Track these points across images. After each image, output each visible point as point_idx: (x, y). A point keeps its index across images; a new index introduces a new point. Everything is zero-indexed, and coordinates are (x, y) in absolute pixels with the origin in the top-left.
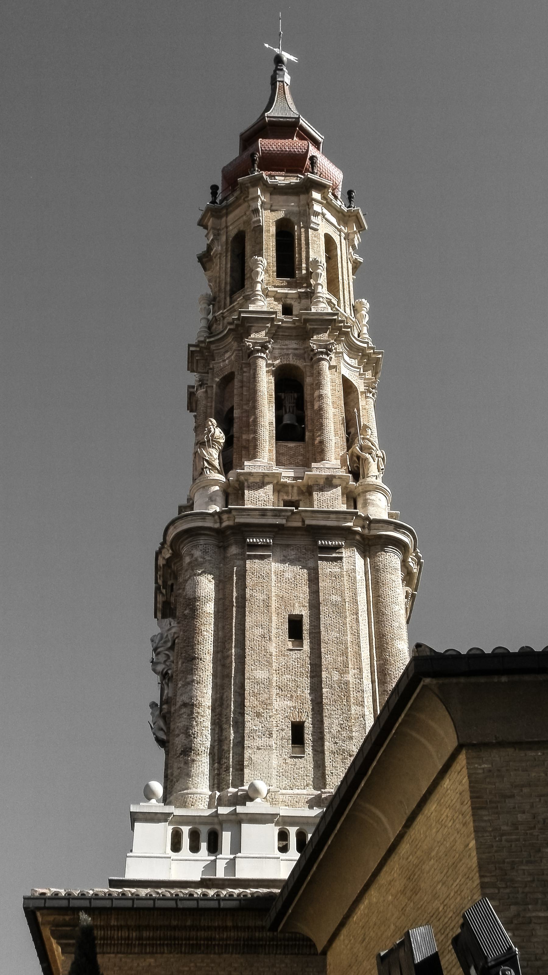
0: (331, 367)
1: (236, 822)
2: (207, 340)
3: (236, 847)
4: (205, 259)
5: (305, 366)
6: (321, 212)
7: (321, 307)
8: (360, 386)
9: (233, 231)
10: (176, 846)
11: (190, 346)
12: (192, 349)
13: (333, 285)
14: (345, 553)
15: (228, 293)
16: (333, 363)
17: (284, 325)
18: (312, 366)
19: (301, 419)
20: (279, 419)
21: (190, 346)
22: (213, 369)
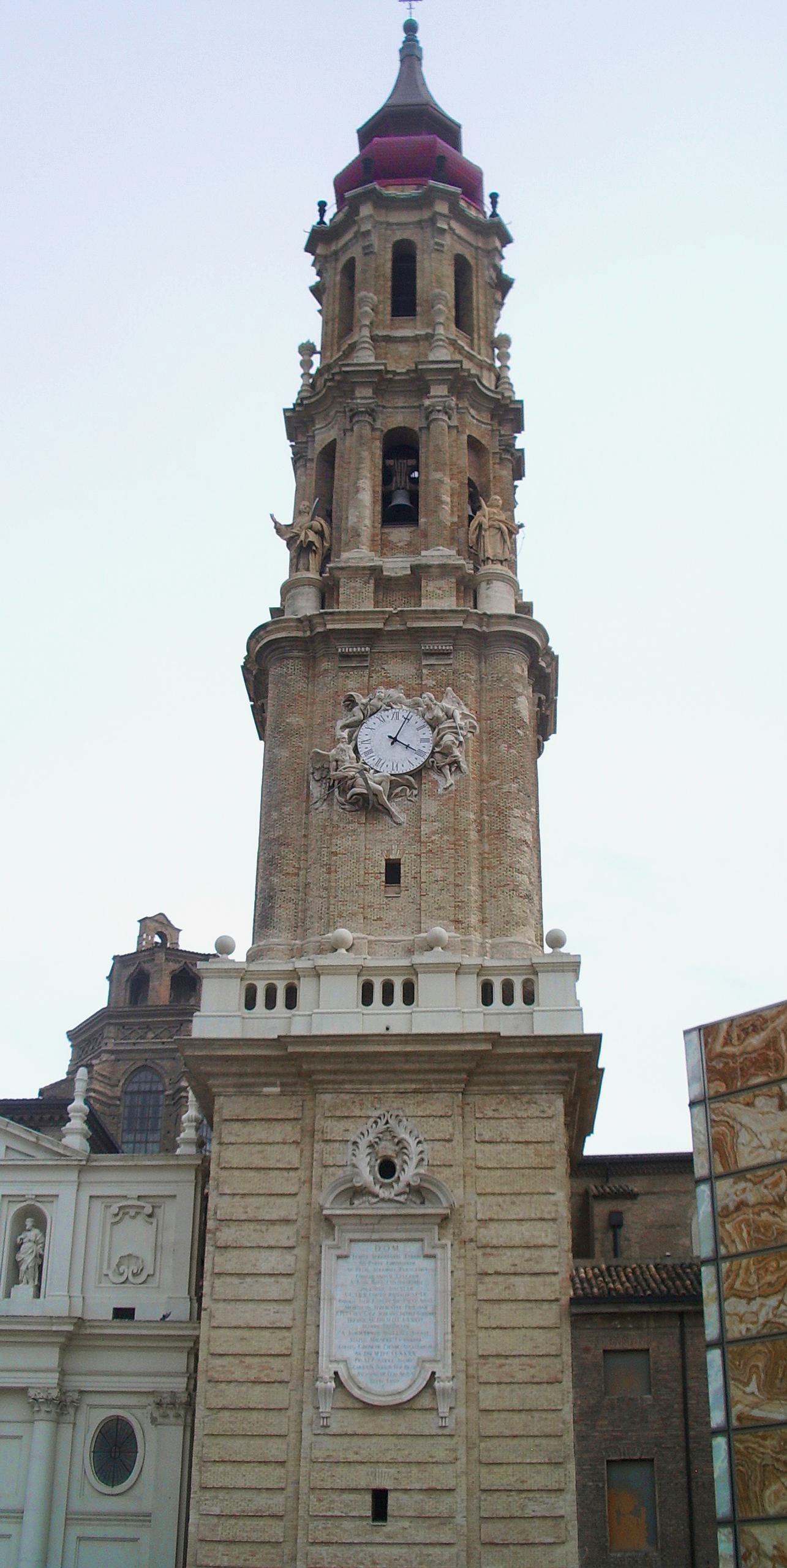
0: (449, 427)
2: (305, 402)
4: (317, 291)
5: (421, 429)
6: (446, 227)
7: (442, 354)
9: (344, 259)
10: (250, 1004)
11: (285, 410)
12: (288, 414)
13: (462, 319)
15: (335, 340)
16: (454, 422)
17: (397, 378)
18: (428, 428)
19: (414, 497)
20: (386, 498)
21: (285, 410)
22: (314, 437)
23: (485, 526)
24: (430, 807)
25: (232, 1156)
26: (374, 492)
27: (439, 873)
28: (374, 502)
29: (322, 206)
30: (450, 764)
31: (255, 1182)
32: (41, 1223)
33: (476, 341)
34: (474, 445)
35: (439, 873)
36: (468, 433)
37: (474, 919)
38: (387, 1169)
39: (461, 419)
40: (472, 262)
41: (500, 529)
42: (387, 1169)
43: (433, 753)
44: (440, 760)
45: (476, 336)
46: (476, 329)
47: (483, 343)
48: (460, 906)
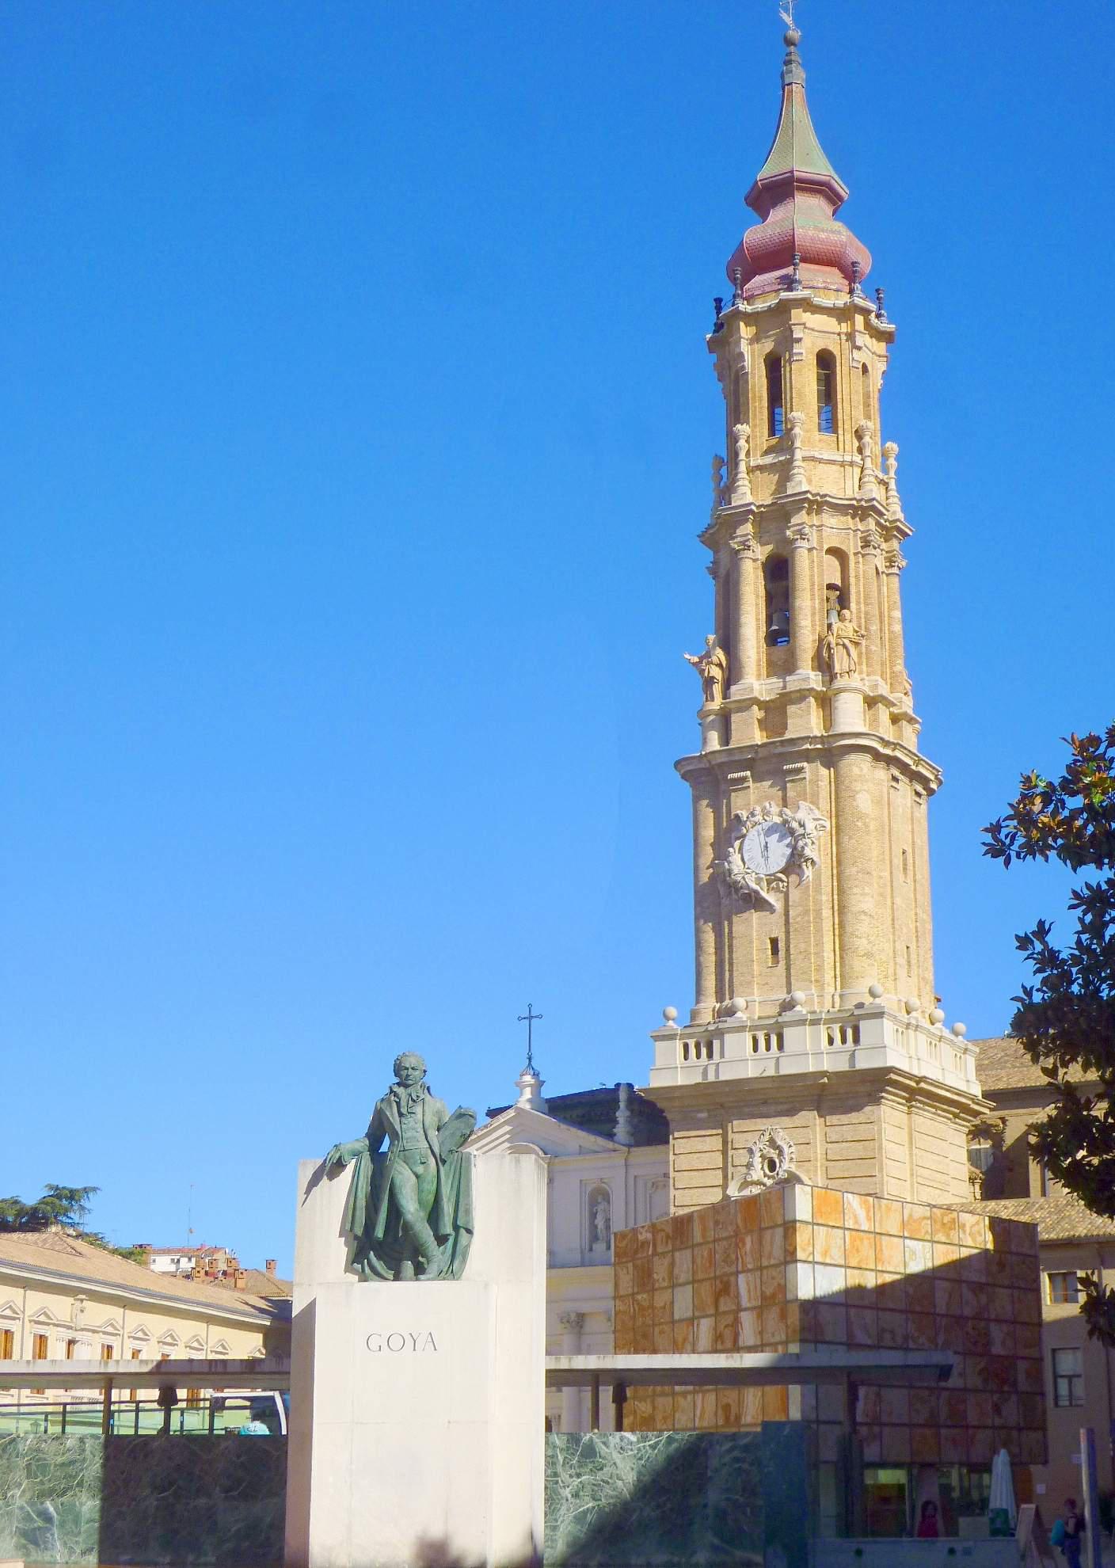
1: (720, 1034)
3: (722, 1055)
8: (851, 546)
14: (807, 775)
23: (833, 645)
24: (795, 894)
25: (683, 1162)
26: (758, 620)
27: (802, 946)
28: (758, 628)
29: (718, 301)
31: (697, 1179)
32: (607, 1197)
33: (841, 438)
34: (834, 552)
35: (802, 946)
36: (826, 547)
37: (829, 976)
38: (772, 1166)
39: (820, 538)
40: (836, 352)
41: (844, 646)
42: (772, 1166)
44: (795, 862)
45: (840, 432)
46: (840, 424)
47: (848, 436)
48: (820, 969)
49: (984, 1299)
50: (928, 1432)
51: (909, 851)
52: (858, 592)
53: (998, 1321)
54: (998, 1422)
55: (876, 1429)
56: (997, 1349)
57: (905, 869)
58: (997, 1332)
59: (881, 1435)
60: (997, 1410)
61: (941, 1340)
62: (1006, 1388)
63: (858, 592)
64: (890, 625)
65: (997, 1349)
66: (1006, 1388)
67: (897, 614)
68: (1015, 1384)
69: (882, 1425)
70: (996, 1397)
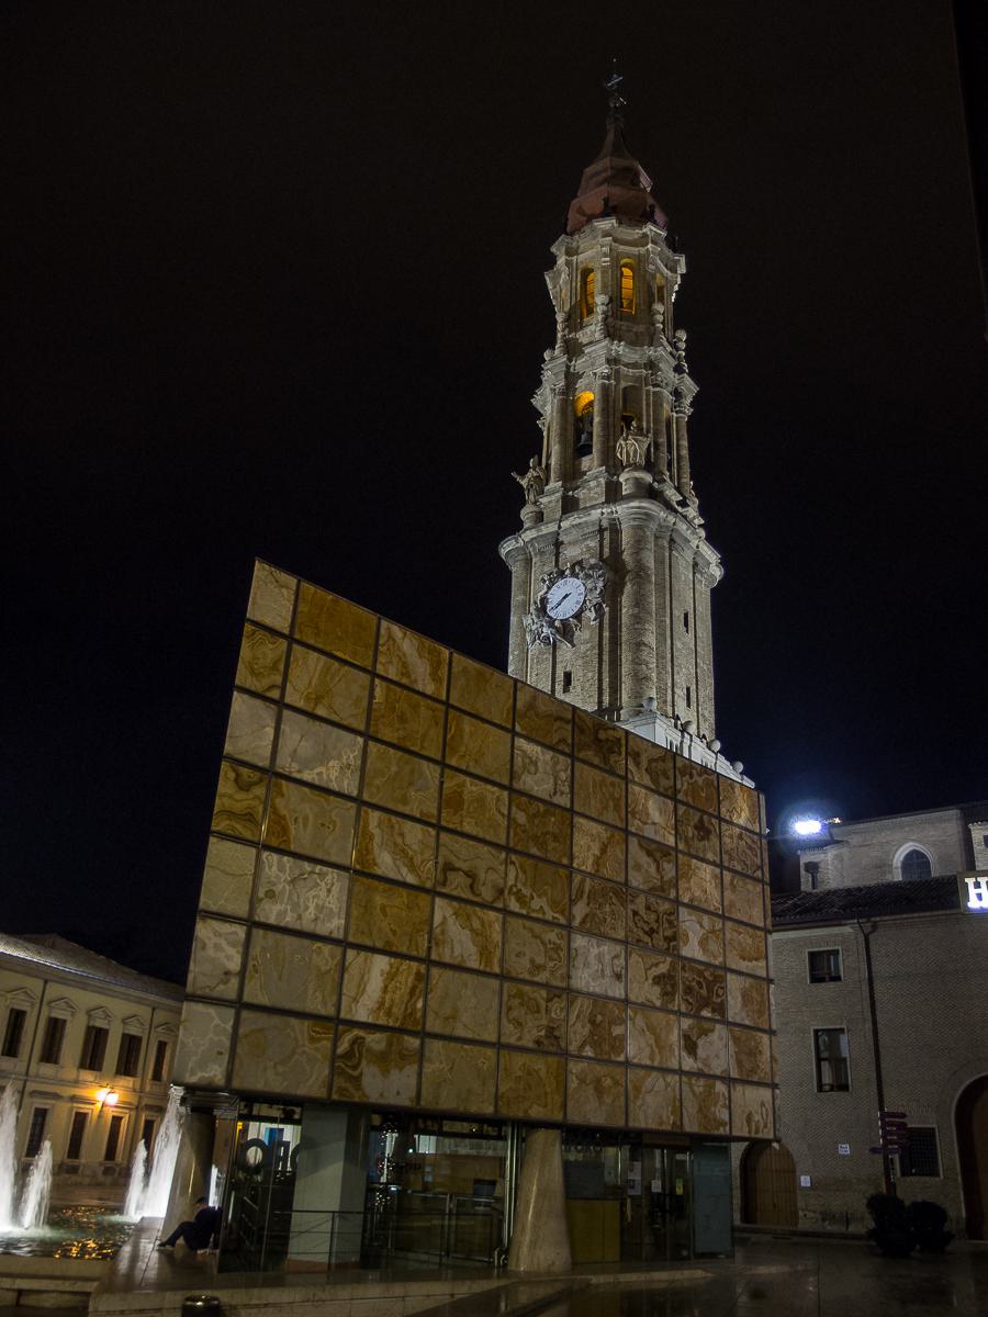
30: (594, 606)
43: (585, 601)
49: (669, 870)
50: (540, 1064)
51: (692, 611)
52: (648, 415)
53: (690, 906)
54: (689, 1064)
55: (413, 1043)
56: (691, 950)
57: (686, 624)
58: (689, 922)
59: (421, 1056)
60: (691, 1047)
61: (580, 911)
62: (706, 1013)
63: (648, 415)
64: (678, 450)
65: (691, 950)
66: (706, 1013)
67: (685, 443)
68: (721, 1009)
69: (424, 1035)
70: (686, 1023)
